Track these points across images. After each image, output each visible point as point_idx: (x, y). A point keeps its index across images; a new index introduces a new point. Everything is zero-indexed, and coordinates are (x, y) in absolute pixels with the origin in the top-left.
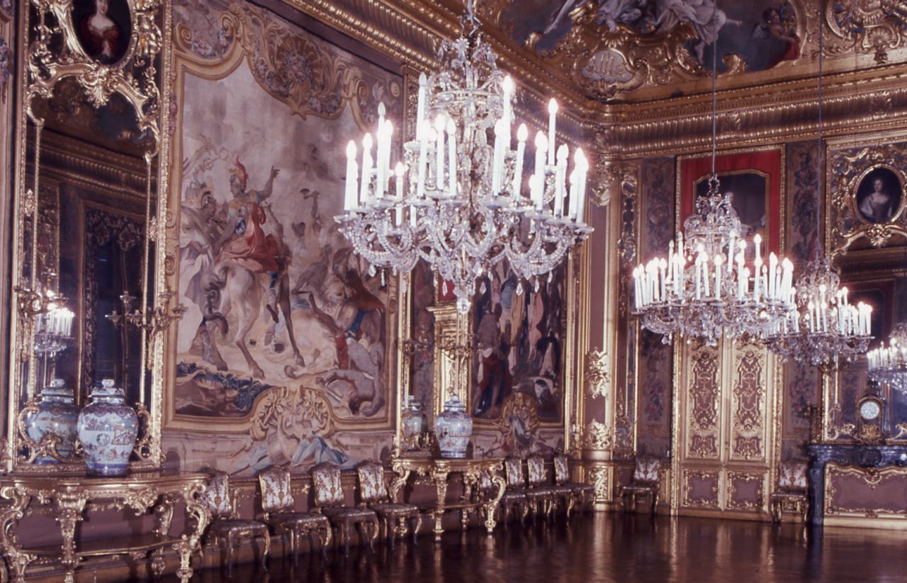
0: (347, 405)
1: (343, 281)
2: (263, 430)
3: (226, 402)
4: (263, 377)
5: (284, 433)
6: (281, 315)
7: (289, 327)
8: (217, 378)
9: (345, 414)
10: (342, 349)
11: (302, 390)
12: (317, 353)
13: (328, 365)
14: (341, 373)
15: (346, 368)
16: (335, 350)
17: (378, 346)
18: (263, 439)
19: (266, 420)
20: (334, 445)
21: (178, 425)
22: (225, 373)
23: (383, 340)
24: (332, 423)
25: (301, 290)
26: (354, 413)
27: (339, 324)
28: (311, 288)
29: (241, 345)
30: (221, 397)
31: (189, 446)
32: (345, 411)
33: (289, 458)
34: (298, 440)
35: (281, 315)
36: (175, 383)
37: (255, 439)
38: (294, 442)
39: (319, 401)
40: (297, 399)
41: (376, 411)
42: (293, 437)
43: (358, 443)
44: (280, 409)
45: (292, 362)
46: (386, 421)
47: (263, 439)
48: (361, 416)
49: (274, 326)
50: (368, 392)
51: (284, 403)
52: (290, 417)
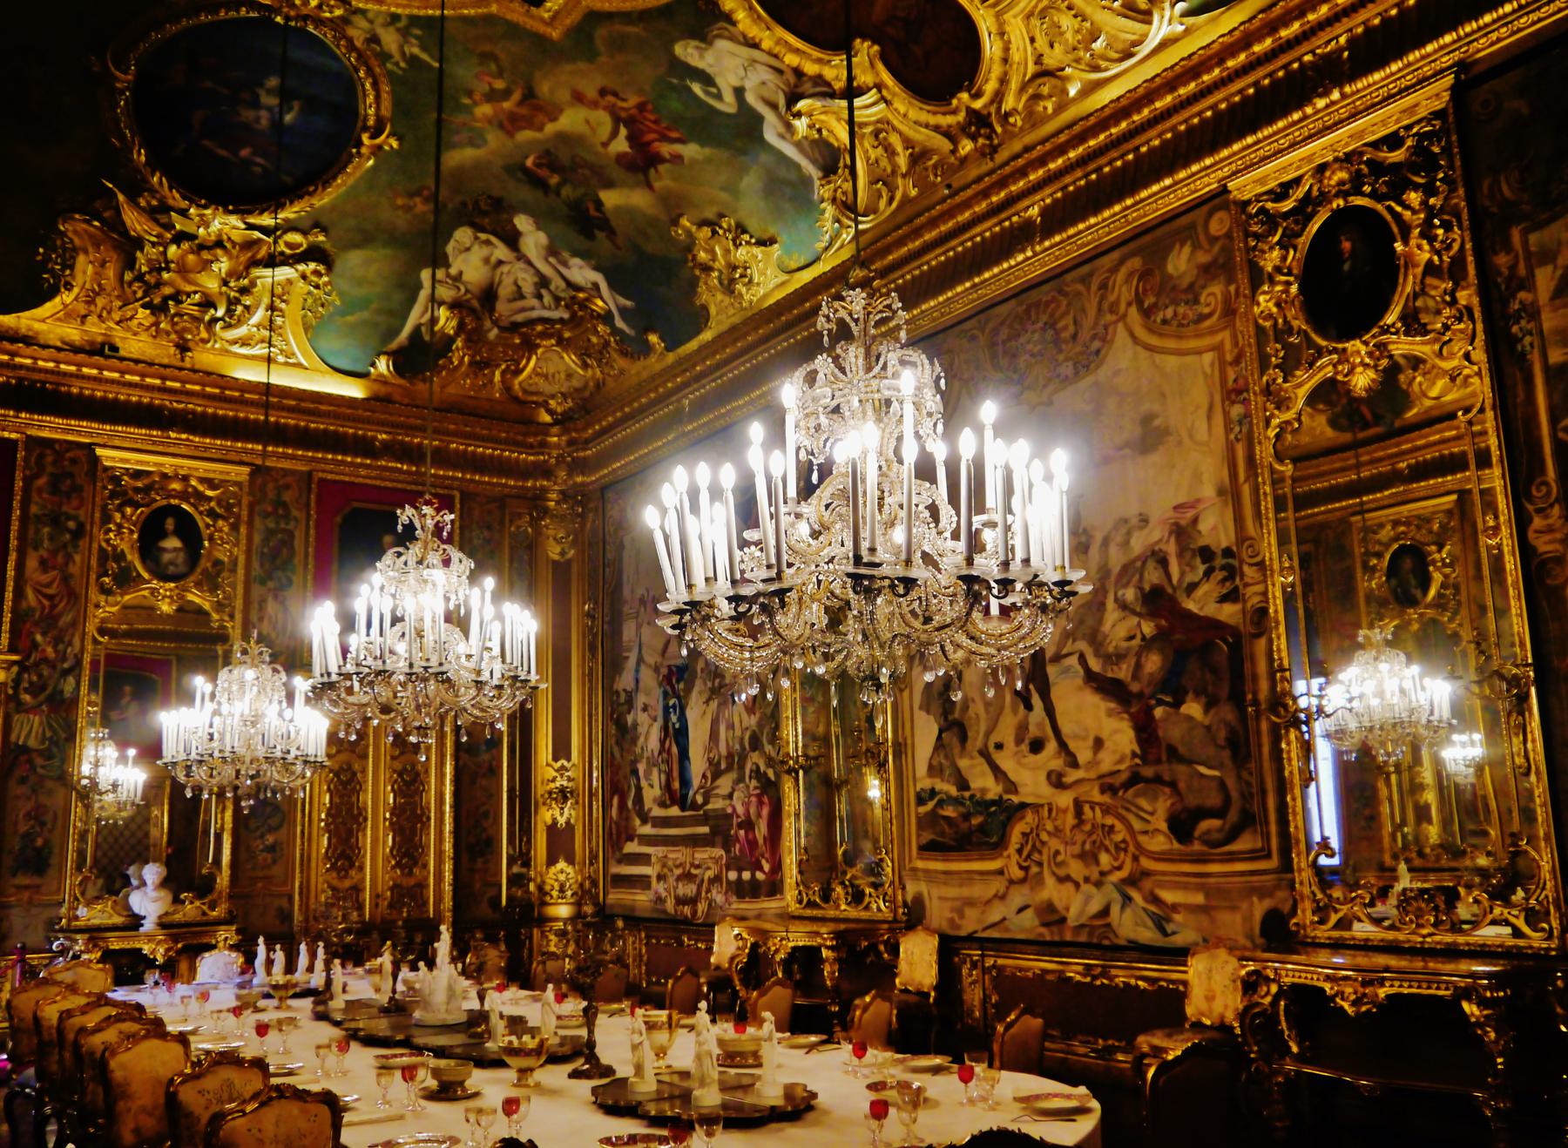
0: (1163, 826)
1: (1134, 613)
2: (1021, 867)
3: (971, 832)
4: (1016, 792)
5: (1054, 874)
6: (1036, 700)
7: (1050, 711)
8: (957, 801)
9: (1159, 843)
10: (1145, 729)
11: (1078, 806)
12: (1098, 743)
13: (1120, 761)
14: (1148, 772)
15: (1158, 761)
16: (1131, 734)
17: (1227, 713)
18: (1023, 881)
19: (1025, 853)
20: (1145, 899)
21: (920, 864)
22: (967, 794)
23: (1237, 698)
24: (1136, 859)
25: (1065, 651)
26: (1180, 842)
27: (1135, 687)
28: (1082, 645)
29: (984, 753)
30: (965, 826)
31: (935, 892)
32: (1161, 838)
33: (1064, 913)
34: (1077, 885)
35: (1036, 700)
36: (917, 814)
37: (1011, 882)
38: (1070, 886)
39: (1109, 821)
40: (1070, 820)
41: (1232, 836)
42: (1068, 878)
43: (1199, 899)
44: (1044, 836)
45: (1057, 764)
46: (1268, 856)
47: (1023, 881)
48: (1197, 847)
49: (1026, 717)
50: (1214, 800)
51: (1049, 826)
52: (1061, 849)
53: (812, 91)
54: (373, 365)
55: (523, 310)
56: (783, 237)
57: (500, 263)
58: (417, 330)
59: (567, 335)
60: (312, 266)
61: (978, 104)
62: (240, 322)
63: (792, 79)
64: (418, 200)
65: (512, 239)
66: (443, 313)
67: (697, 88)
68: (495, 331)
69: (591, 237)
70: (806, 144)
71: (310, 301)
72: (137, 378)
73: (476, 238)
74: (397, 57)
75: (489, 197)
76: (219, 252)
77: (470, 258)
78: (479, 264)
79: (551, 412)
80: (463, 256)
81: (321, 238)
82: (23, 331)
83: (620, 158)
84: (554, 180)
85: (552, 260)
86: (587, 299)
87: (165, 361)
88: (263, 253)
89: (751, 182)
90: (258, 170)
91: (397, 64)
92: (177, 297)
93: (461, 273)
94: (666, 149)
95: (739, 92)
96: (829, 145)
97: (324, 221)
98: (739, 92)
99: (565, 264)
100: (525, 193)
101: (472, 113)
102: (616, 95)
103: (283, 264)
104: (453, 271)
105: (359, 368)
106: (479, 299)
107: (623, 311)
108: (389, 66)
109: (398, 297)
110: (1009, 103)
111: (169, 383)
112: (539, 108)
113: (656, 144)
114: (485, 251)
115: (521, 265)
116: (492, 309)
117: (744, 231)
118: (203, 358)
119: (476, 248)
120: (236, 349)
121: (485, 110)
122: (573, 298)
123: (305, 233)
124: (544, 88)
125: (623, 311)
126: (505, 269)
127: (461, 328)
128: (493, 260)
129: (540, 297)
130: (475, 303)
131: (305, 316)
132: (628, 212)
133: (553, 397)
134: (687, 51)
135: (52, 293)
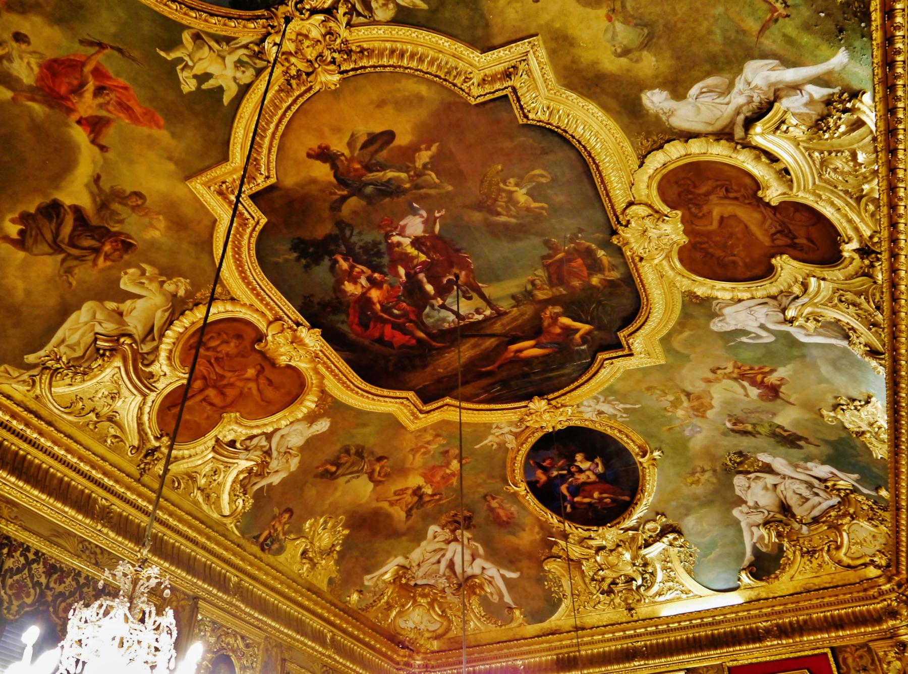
53: (788, 302)
54: (739, 579)
55: (814, 507)
56: (872, 392)
57: (775, 486)
58: (754, 547)
59: (851, 511)
60: (671, 536)
61: (855, 245)
62: (652, 584)
63: (775, 303)
64: (697, 475)
65: (768, 469)
66: (763, 531)
67: (744, 339)
68: (805, 528)
69: (800, 447)
70: (821, 330)
71: (682, 556)
72: (632, 632)
73: (749, 479)
74: (619, 414)
75: (735, 453)
76: (620, 549)
77: (757, 493)
78: (763, 492)
79: (878, 567)
80: (749, 491)
81: (664, 520)
82: (555, 628)
83: (761, 396)
84: (750, 428)
85: (799, 470)
86: (834, 485)
87: (624, 620)
88: (641, 541)
89: (826, 370)
90: (608, 500)
91: (621, 417)
92: (614, 583)
93: (756, 503)
94: (773, 379)
95: (762, 327)
96: (830, 323)
97: (660, 512)
98: (762, 327)
99: (807, 469)
100: (745, 443)
101: (678, 418)
102: (719, 369)
103: (654, 542)
104: (751, 503)
105: (732, 585)
106: (779, 513)
107: (857, 481)
108: (620, 420)
109: (731, 532)
110: (867, 233)
111: (627, 633)
112: (699, 398)
113: (765, 379)
114: (760, 484)
115: (788, 481)
116: (794, 516)
117: (854, 400)
118: (643, 611)
119: (753, 484)
120: (658, 599)
121: (680, 413)
122: (827, 487)
123: (654, 521)
124: (689, 388)
125: (857, 481)
126: (781, 487)
127: (779, 535)
128: (769, 486)
129: (817, 494)
130: (779, 516)
131: (685, 566)
132: (796, 423)
133: (874, 555)
134: (717, 326)
135: (560, 601)
